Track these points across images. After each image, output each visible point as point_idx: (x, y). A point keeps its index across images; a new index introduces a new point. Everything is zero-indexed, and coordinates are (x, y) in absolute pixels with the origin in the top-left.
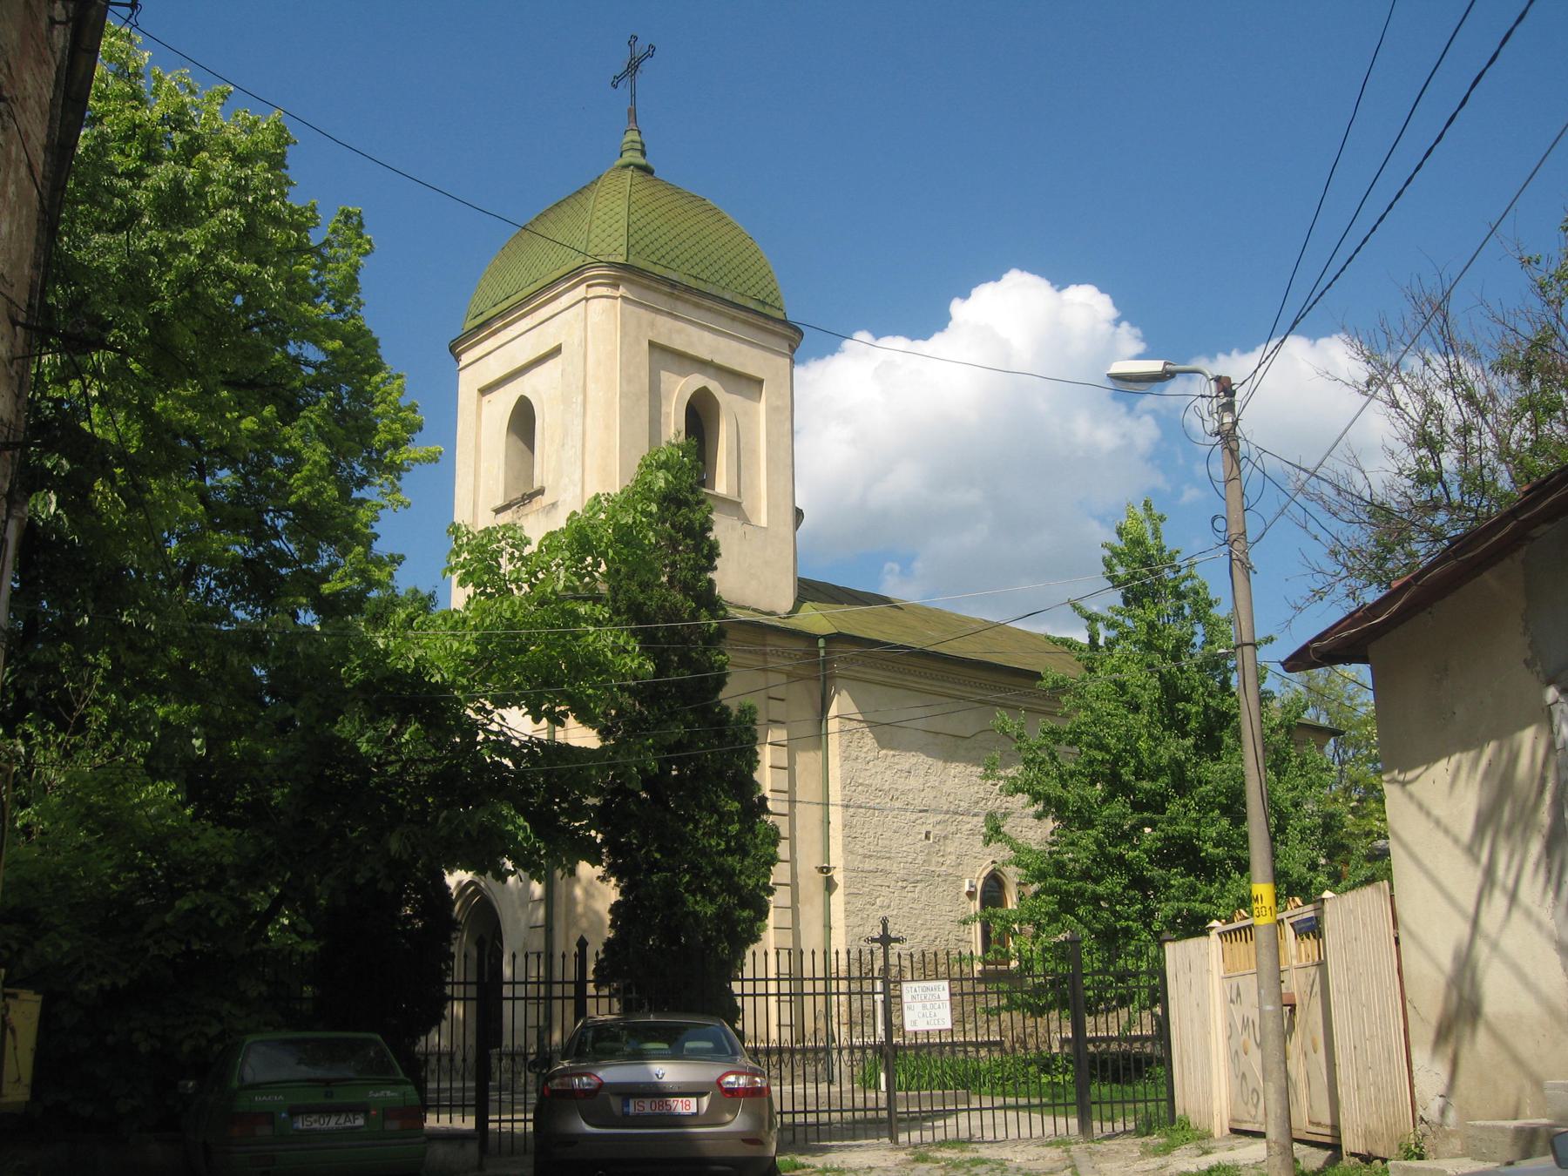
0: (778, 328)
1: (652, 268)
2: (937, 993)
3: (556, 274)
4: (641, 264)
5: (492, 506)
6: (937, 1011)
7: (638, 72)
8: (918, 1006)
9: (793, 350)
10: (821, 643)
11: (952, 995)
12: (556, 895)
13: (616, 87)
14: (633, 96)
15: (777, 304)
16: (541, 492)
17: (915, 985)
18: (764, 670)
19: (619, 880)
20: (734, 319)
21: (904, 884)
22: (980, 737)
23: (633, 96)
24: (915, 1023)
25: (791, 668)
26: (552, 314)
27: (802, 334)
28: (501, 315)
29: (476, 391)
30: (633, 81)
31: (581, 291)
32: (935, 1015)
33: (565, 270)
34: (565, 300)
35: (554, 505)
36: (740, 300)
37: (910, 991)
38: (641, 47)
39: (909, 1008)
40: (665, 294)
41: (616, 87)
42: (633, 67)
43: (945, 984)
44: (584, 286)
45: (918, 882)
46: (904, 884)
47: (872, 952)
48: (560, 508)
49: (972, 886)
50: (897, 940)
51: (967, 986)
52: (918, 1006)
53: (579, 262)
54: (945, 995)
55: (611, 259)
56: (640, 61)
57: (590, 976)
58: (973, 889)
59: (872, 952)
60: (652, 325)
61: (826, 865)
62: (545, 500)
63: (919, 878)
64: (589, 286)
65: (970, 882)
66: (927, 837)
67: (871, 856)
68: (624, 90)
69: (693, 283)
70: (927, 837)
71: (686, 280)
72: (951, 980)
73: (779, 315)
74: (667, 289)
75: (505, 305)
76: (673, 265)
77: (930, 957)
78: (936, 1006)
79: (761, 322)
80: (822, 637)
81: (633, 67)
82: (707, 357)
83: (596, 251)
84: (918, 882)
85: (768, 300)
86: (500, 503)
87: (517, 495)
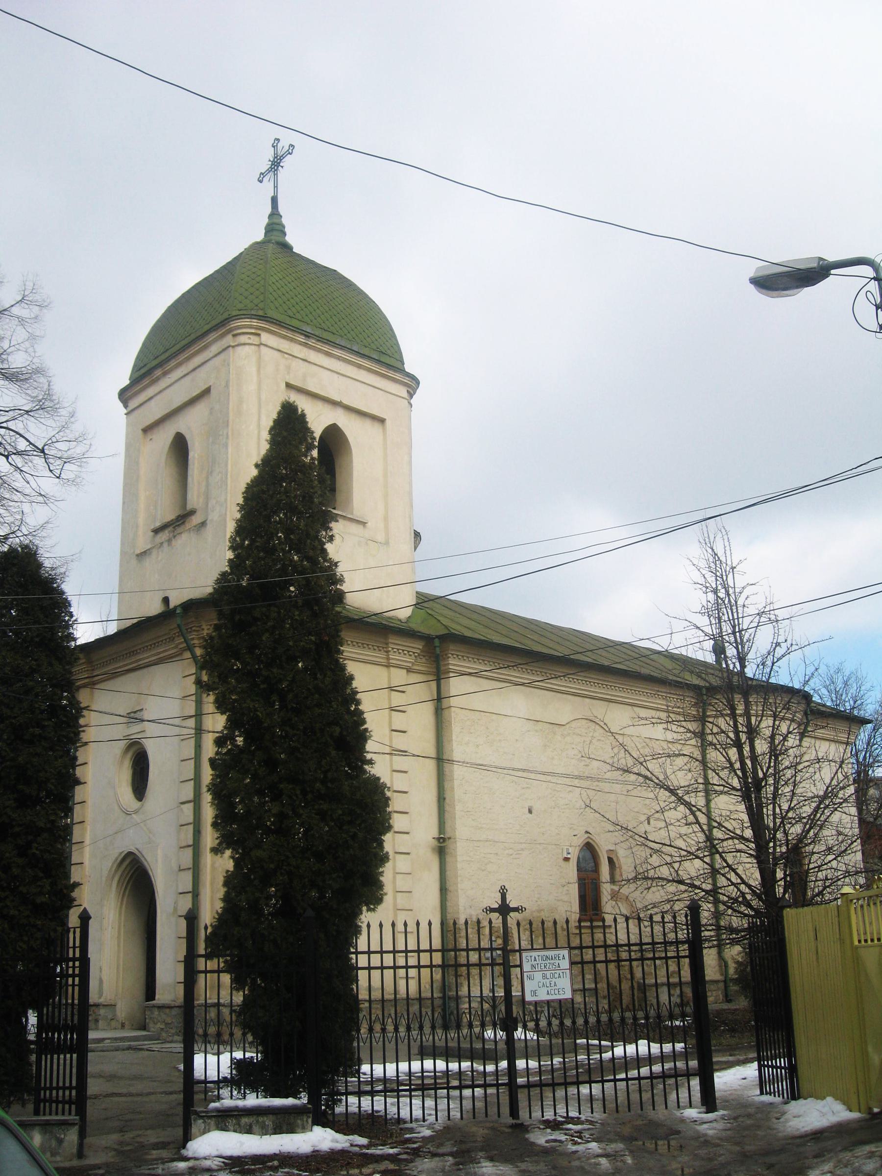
0: (398, 376)
1: (288, 320)
2: (557, 962)
3: (207, 327)
4: (280, 317)
5: (152, 527)
6: (557, 981)
7: (280, 168)
8: (538, 976)
9: (411, 396)
10: (437, 642)
11: (572, 963)
12: (202, 866)
13: (261, 182)
14: (276, 187)
15: (396, 356)
16: (192, 512)
17: (534, 954)
18: (388, 666)
19: (235, 850)
20: (360, 367)
21: (511, 852)
22: (574, 724)
23: (276, 187)
24: (534, 993)
25: (410, 665)
26: (203, 361)
27: (418, 383)
28: (160, 365)
29: (140, 432)
30: (276, 175)
31: (228, 340)
32: (555, 985)
33: (214, 323)
34: (214, 349)
35: (203, 524)
36: (366, 351)
37: (529, 960)
38: (284, 144)
39: (529, 978)
40: (301, 343)
41: (261, 182)
42: (276, 164)
43: (565, 952)
44: (230, 337)
45: (522, 850)
46: (511, 852)
47: (490, 922)
48: (209, 526)
49: (569, 853)
50: (516, 910)
51: (588, 955)
52: (538, 976)
53: (225, 316)
54: (565, 964)
55: (253, 312)
56: (282, 157)
57: (201, 949)
58: (569, 856)
59: (490, 922)
60: (288, 368)
61: (442, 836)
62: (196, 520)
63: (523, 846)
64: (234, 336)
65: (568, 849)
66: (530, 811)
67: (482, 828)
68: (267, 187)
69: (325, 335)
70: (530, 811)
71: (318, 332)
72: (571, 948)
73: (398, 365)
74: (301, 339)
75: (163, 357)
76: (306, 319)
77: (549, 925)
78: (557, 976)
79: (383, 370)
80: (437, 637)
81: (276, 164)
82: (337, 398)
83: (240, 306)
84: (522, 850)
85: (389, 352)
86: (158, 524)
87: (170, 517)
